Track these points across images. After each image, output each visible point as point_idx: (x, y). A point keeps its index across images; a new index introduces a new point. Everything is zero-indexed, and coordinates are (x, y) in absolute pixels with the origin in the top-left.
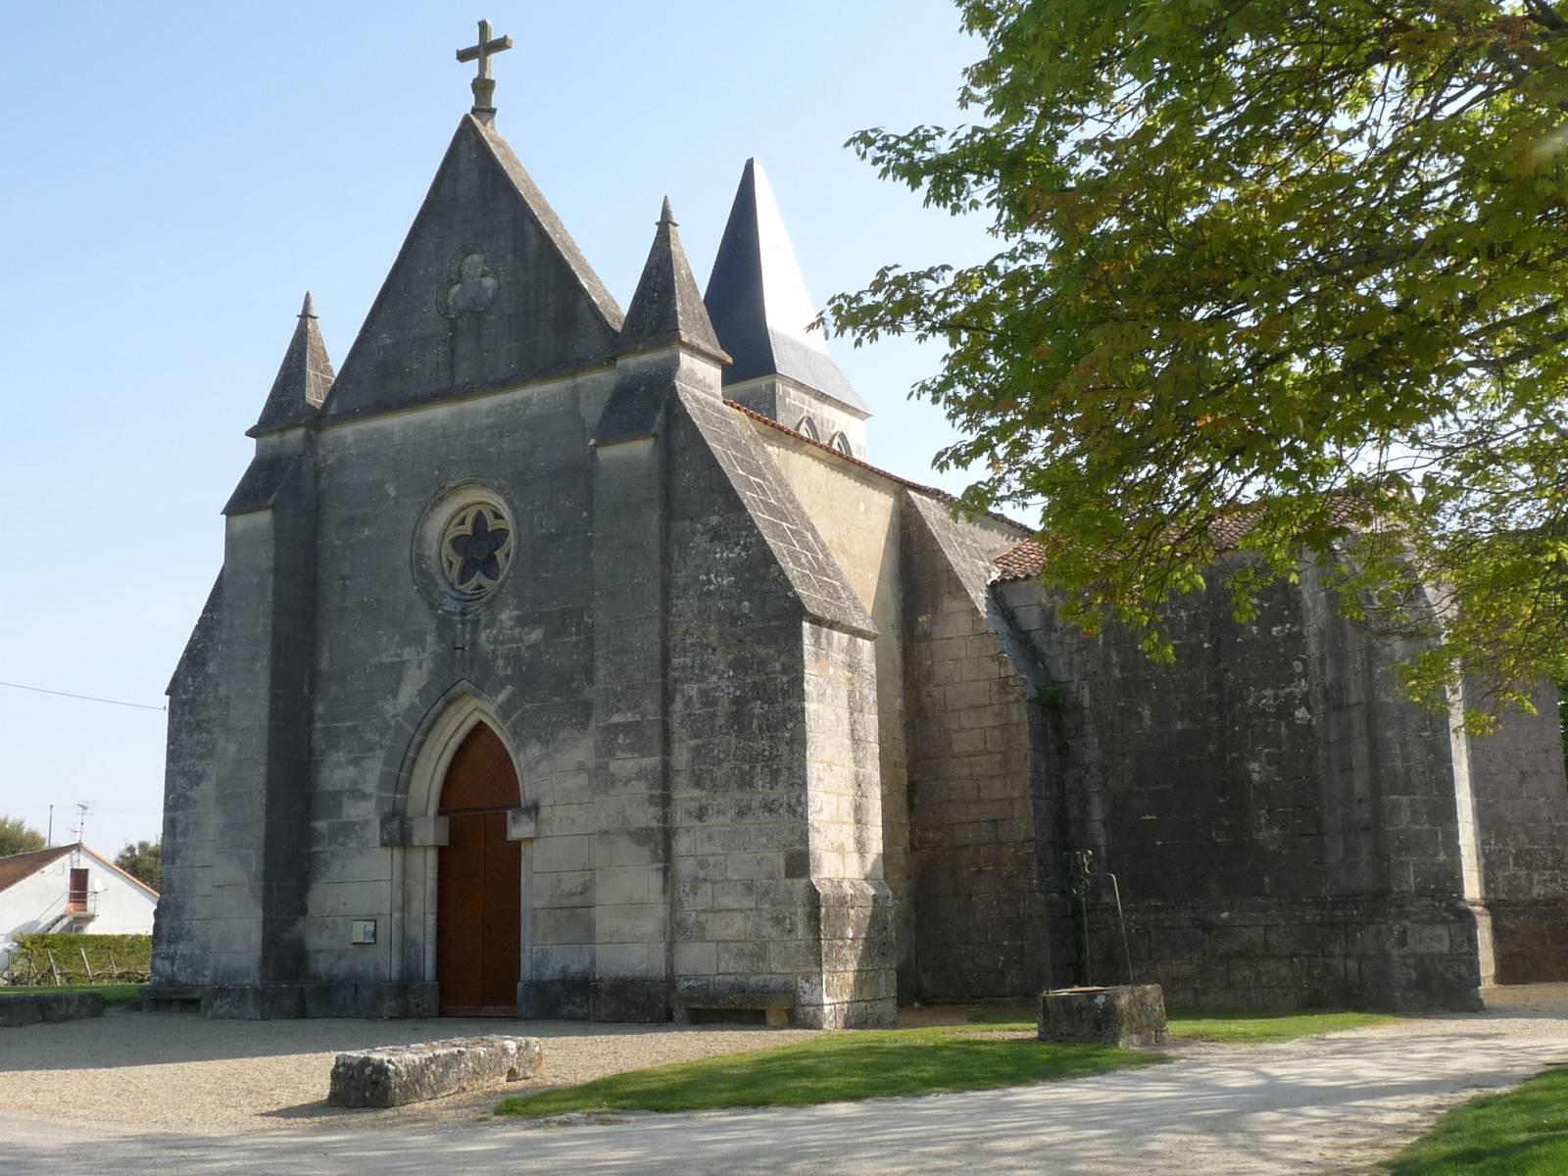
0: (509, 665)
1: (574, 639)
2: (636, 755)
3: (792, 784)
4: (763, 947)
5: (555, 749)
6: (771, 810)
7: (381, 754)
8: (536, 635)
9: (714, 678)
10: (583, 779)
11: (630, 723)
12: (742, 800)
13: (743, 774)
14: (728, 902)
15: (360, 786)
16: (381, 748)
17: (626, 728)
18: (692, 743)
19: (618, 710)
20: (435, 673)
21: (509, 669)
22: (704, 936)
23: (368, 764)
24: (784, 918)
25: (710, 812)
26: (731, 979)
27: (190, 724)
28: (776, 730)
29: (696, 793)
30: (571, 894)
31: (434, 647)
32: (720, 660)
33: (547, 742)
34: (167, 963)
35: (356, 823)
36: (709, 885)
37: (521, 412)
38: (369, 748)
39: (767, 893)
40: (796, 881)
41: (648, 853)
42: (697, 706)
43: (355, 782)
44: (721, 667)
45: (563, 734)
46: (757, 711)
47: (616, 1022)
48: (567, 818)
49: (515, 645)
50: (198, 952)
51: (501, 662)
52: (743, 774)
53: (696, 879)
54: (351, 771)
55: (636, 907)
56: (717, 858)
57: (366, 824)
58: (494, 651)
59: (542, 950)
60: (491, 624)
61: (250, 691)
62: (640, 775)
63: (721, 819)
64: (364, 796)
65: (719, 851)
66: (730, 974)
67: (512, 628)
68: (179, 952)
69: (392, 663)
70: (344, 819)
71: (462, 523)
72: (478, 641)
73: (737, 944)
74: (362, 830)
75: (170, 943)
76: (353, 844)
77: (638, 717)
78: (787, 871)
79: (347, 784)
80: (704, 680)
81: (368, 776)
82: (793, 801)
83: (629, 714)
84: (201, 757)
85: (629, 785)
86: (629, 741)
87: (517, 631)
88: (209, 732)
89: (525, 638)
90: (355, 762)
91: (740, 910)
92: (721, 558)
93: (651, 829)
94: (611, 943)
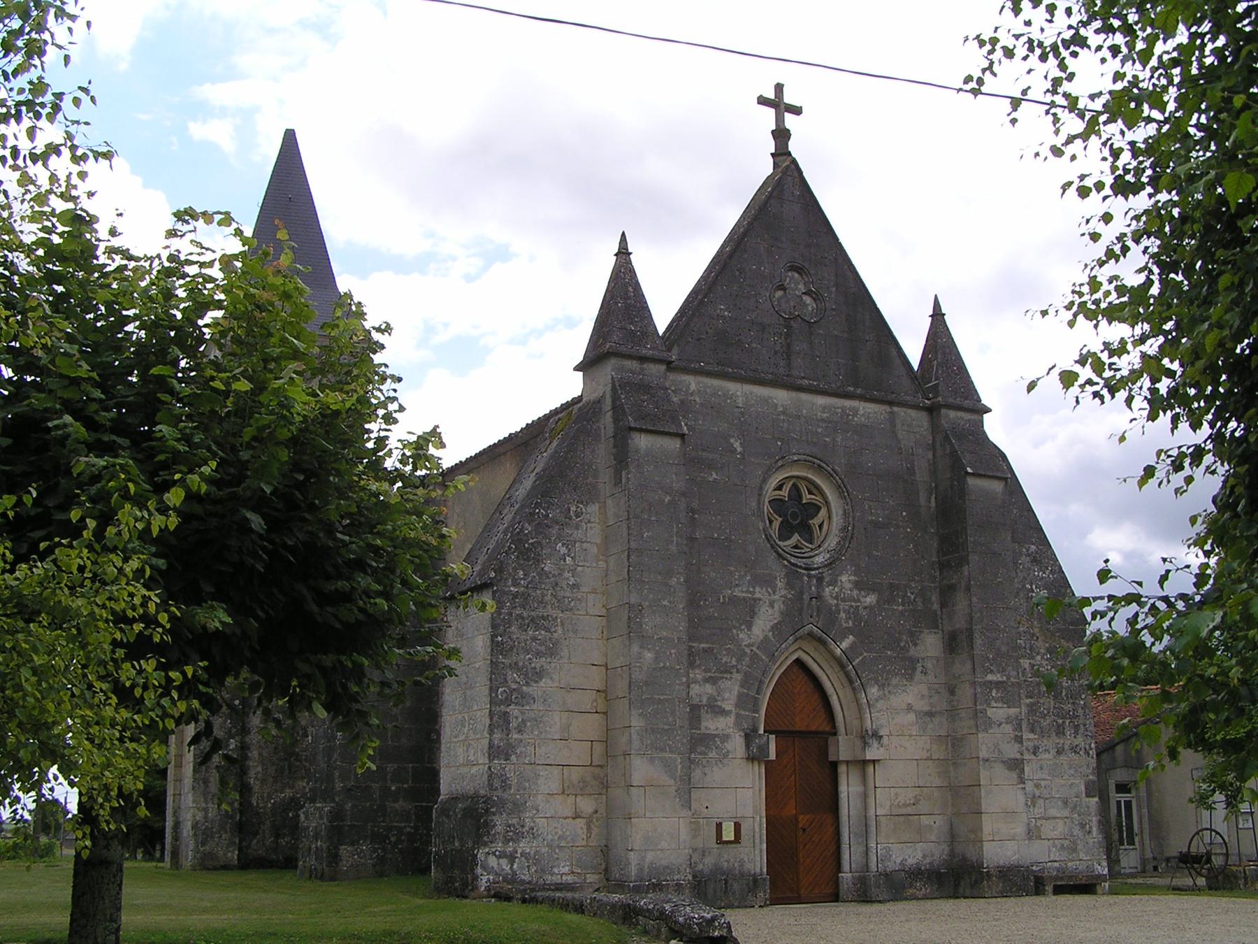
0: (850, 618)
1: (900, 608)
2: (1005, 706)
3: (1086, 736)
4: (1075, 843)
5: (889, 692)
6: (1075, 752)
7: (739, 677)
8: (871, 599)
9: (1039, 658)
10: (911, 717)
11: (999, 682)
12: (1059, 743)
13: (1059, 726)
14: (1053, 812)
15: (719, 703)
16: (738, 671)
17: (998, 685)
18: (1028, 701)
19: (992, 672)
20: (786, 614)
21: (850, 622)
22: (1040, 836)
23: (724, 684)
24: (1085, 825)
25: (1041, 750)
26: (1056, 864)
27: (523, 618)
28: (1076, 699)
29: (1031, 736)
30: (906, 805)
31: (783, 592)
32: (1042, 645)
33: (883, 685)
34: (504, 862)
35: (715, 736)
36: (1042, 801)
37: (850, 417)
38: (727, 670)
39: (1075, 807)
40: (1091, 799)
41: (1016, 776)
42: (1030, 675)
43: (712, 699)
44: (1042, 651)
45: (895, 681)
46: (1064, 684)
47: (863, 901)
48: (901, 746)
49: (853, 604)
50: (544, 850)
51: (843, 615)
52: (1059, 726)
53: (1034, 796)
54: (709, 688)
55: (1009, 814)
56: (1046, 782)
57: (725, 738)
58: (837, 605)
59: (884, 848)
60: (833, 583)
61: (665, 603)
62: (1008, 720)
63: (1047, 756)
64: (723, 712)
65: (1047, 777)
66: (1055, 861)
67: (851, 590)
68: (519, 851)
69: (744, 599)
70: (703, 730)
71: (810, 493)
72: (824, 594)
73: (1060, 841)
74: (722, 743)
75: (506, 841)
76: (713, 754)
77: (1005, 678)
78: (1086, 793)
79: (704, 701)
80: (1033, 658)
81: (727, 695)
82: (1087, 747)
83: (999, 675)
84: (538, 654)
85: (1001, 727)
86: (999, 695)
87: (855, 592)
88: (547, 630)
89: (862, 600)
90: (713, 681)
91: (1061, 818)
92: (1038, 576)
93: (1016, 759)
94: (993, 840)
